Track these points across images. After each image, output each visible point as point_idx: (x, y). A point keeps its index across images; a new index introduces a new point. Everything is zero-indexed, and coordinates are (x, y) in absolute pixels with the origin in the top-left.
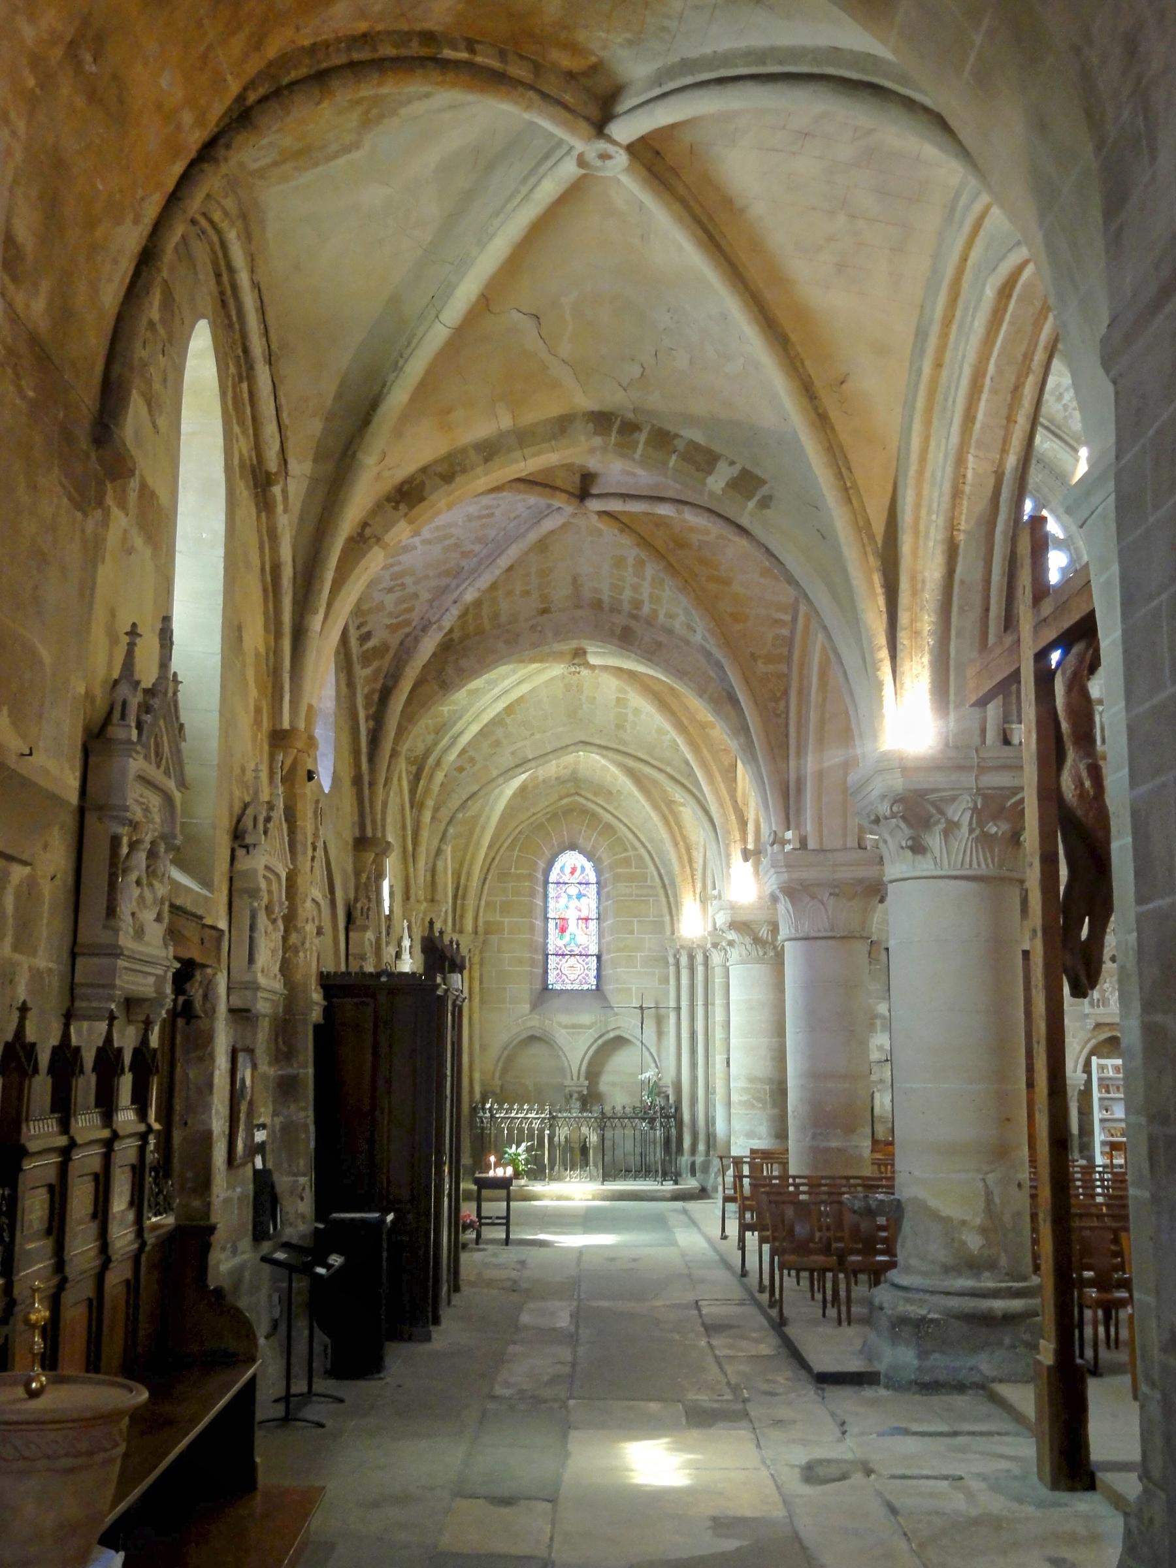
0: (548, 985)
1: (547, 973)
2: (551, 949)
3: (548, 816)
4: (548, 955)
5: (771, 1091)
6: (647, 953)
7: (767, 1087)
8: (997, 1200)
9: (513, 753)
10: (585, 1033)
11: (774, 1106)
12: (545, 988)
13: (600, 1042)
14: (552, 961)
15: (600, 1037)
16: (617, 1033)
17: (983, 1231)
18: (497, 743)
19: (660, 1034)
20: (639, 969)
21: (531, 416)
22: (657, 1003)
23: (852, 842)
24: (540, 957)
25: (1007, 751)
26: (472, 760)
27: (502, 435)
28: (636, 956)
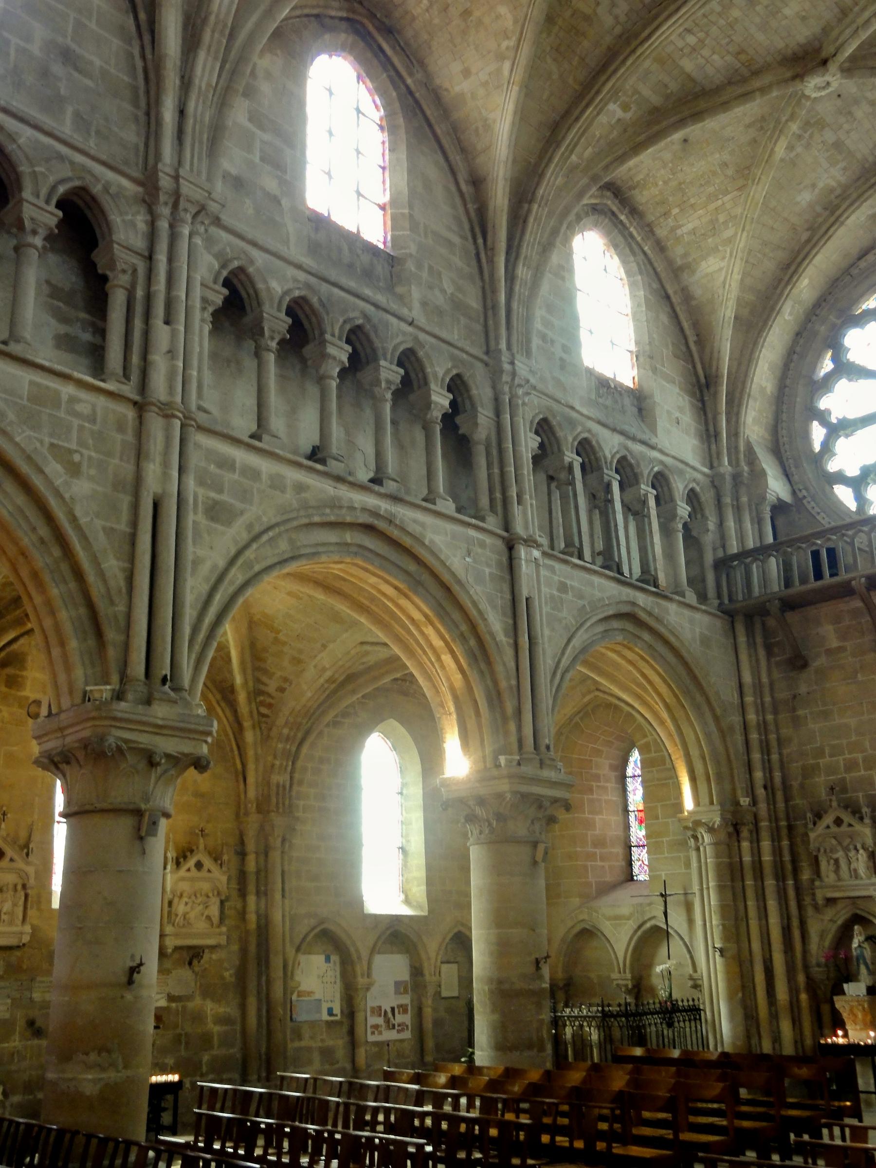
0: (632, 876)
1: (631, 865)
2: (634, 840)
3: (581, 714)
4: (630, 847)
5: (491, 992)
6: (671, 838)
7: (486, 988)
9: (315, 667)
10: (626, 924)
11: (493, 1011)
12: (632, 879)
13: (639, 933)
15: (640, 927)
16: (653, 922)
18: (297, 661)
19: (691, 921)
20: (666, 855)
22: (685, 889)
24: (619, 850)
26: (286, 680)
28: (663, 842)
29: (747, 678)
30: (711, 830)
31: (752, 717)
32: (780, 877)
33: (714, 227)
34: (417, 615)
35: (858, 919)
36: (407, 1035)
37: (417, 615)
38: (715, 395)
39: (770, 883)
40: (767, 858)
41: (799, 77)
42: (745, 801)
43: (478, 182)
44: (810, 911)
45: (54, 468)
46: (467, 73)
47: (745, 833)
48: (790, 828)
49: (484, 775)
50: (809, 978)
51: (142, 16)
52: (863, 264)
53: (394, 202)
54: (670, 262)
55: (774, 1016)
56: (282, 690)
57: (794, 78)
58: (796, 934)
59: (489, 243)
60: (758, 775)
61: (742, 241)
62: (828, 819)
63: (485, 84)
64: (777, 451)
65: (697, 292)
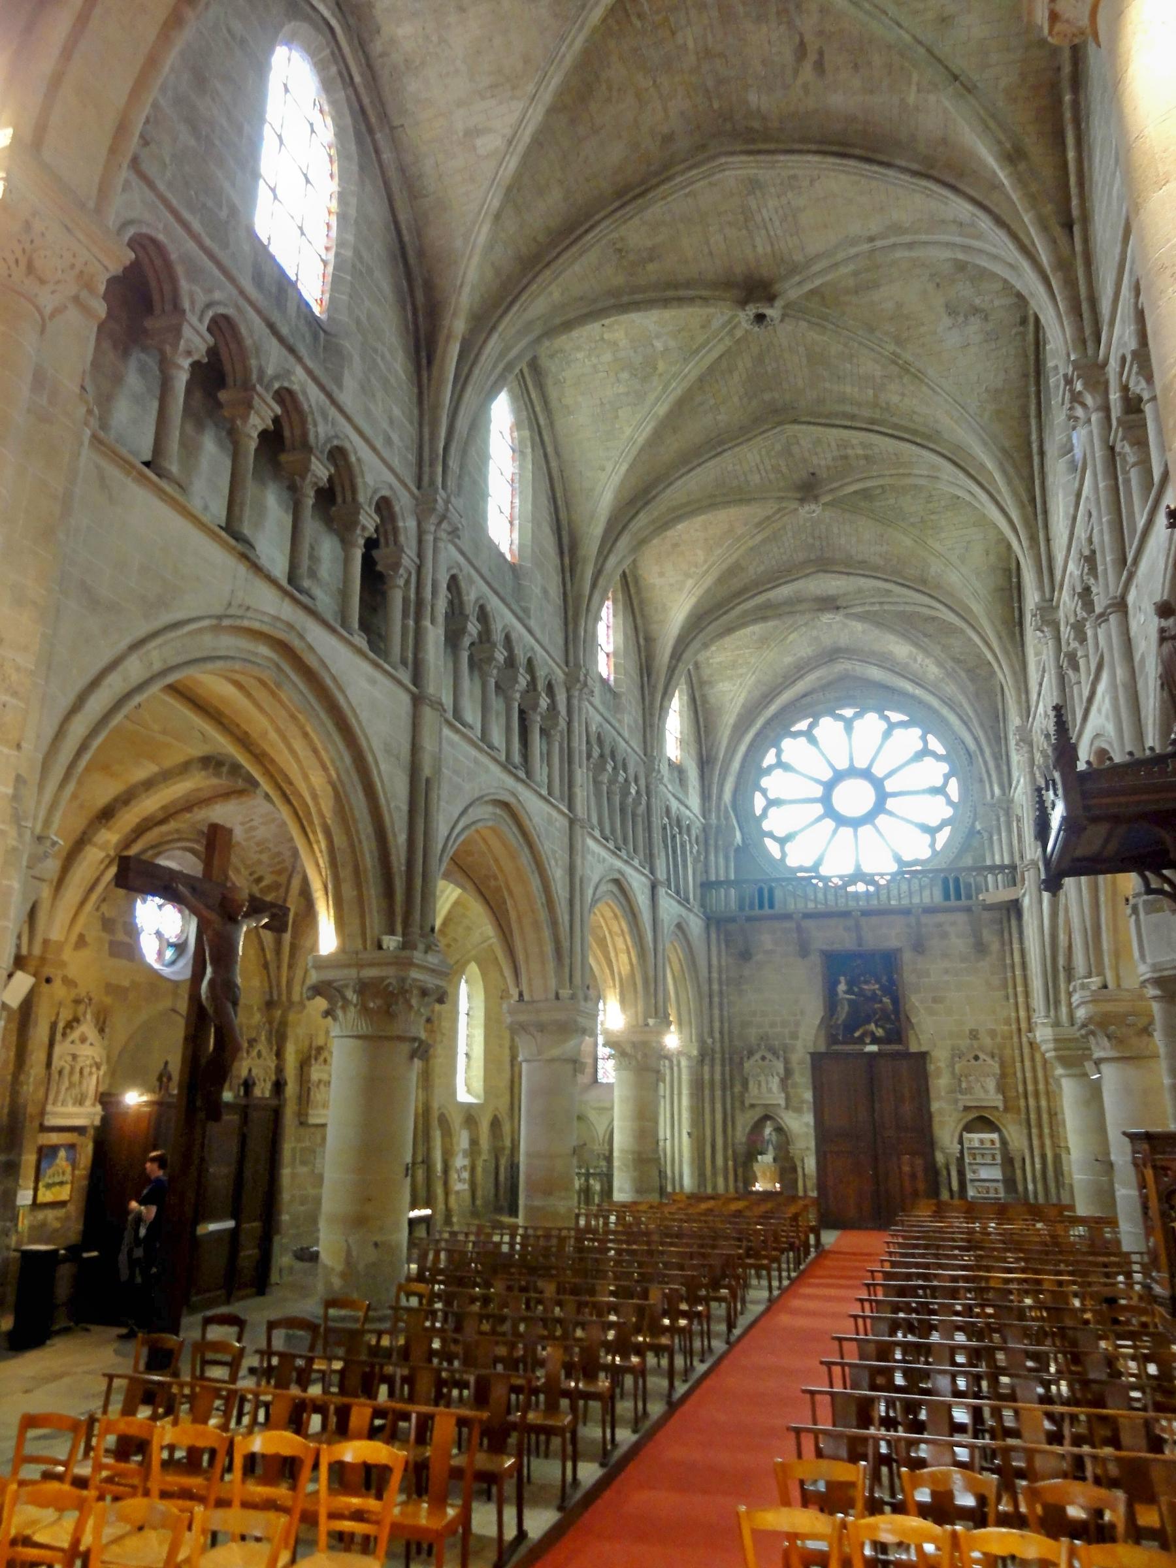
2: (600, 1054)
8: (354, 1253)
12: (595, 1080)
14: (600, 1062)
17: (343, 1275)
18: (469, 928)
21: (168, 763)
23: (552, 996)
25: (378, 954)
26: (455, 940)
27: (156, 775)
29: (715, 961)
30: (689, 1058)
31: (715, 987)
32: (724, 1089)
33: (734, 665)
34: (616, 929)
35: (767, 1117)
36: (466, 1186)
37: (616, 929)
38: (712, 769)
39: (718, 1093)
40: (718, 1077)
41: (821, 610)
42: (709, 1041)
43: (649, 640)
44: (738, 1112)
45: (553, 863)
46: (661, 574)
47: (707, 1060)
48: (731, 1059)
49: (633, 1028)
50: (734, 1152)
51: (567, 561)
52: (804, 701)
53: (615, 654)
54: (699, 677)
55: (714, 1174)
56: (448, 946)
57: (819, 610)
58: (729, 1124)
59: (653, 681)
60: (717, 1025)
61: (750, 680)
62: (757, 1056)
63: (671, 585)
64: (735, 810)
65: (712, 700)
